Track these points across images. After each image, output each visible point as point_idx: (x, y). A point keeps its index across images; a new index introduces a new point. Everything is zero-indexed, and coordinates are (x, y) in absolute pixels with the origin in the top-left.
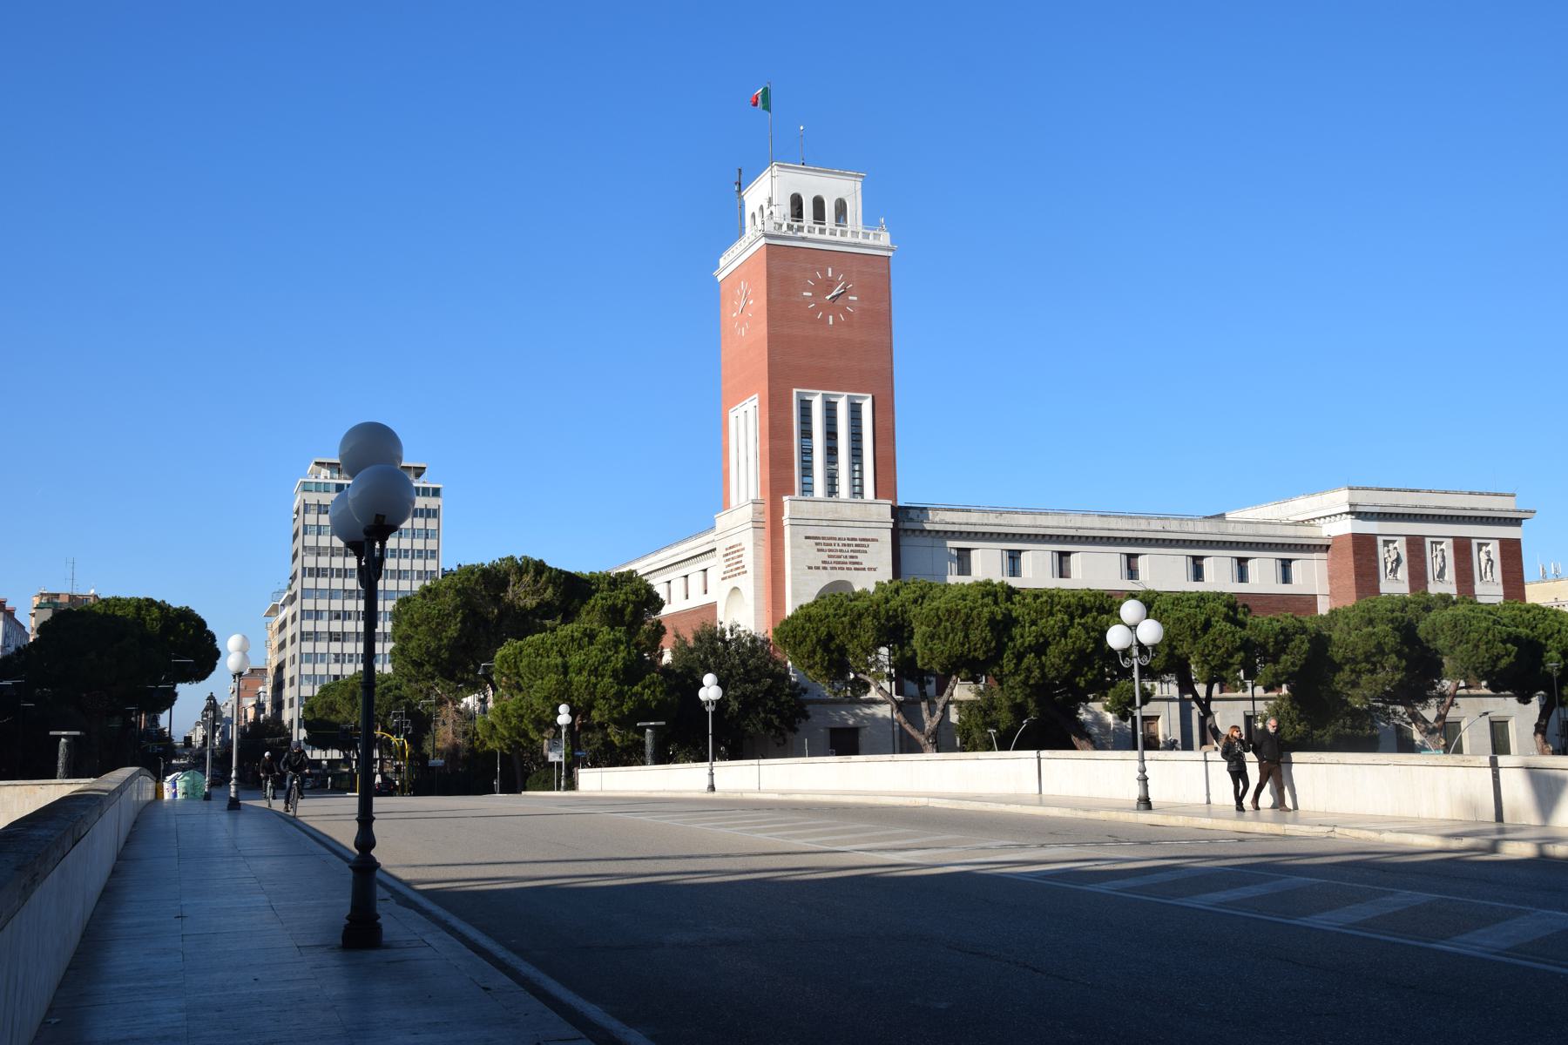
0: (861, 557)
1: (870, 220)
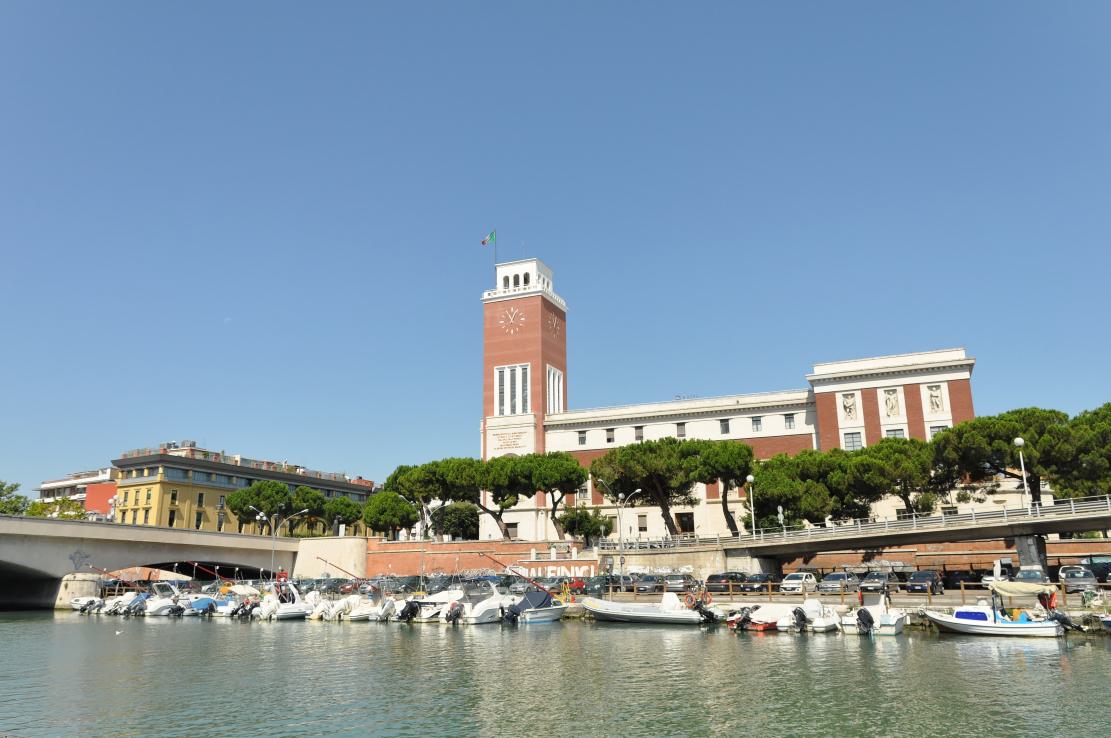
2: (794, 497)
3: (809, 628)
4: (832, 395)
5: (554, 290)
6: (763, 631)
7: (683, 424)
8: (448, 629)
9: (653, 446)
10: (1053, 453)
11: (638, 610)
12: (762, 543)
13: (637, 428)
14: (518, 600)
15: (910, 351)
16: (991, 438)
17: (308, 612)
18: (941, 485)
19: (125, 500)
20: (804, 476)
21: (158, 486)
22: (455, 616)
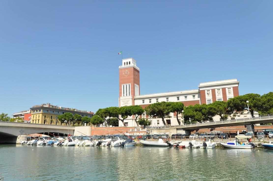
0: (128, 103)
2: (194, 116)
3: (193, 147)
4: (204, 91)
5: (137, 66)
6: (182, 148)
7: (168, 98)
8: (107, 148)
9: (160, 103)
10: (256, 104)
11: (153, 143)
12: (186, 127)
13: (157, 99)
14: (125, 141)
15: (206, 82)
16: (241, 101)
17: (75, 144)
18: (229, 112)
19: (33, 118)
20: (196, 111)
21: (41, 114)
22: (109, 145)
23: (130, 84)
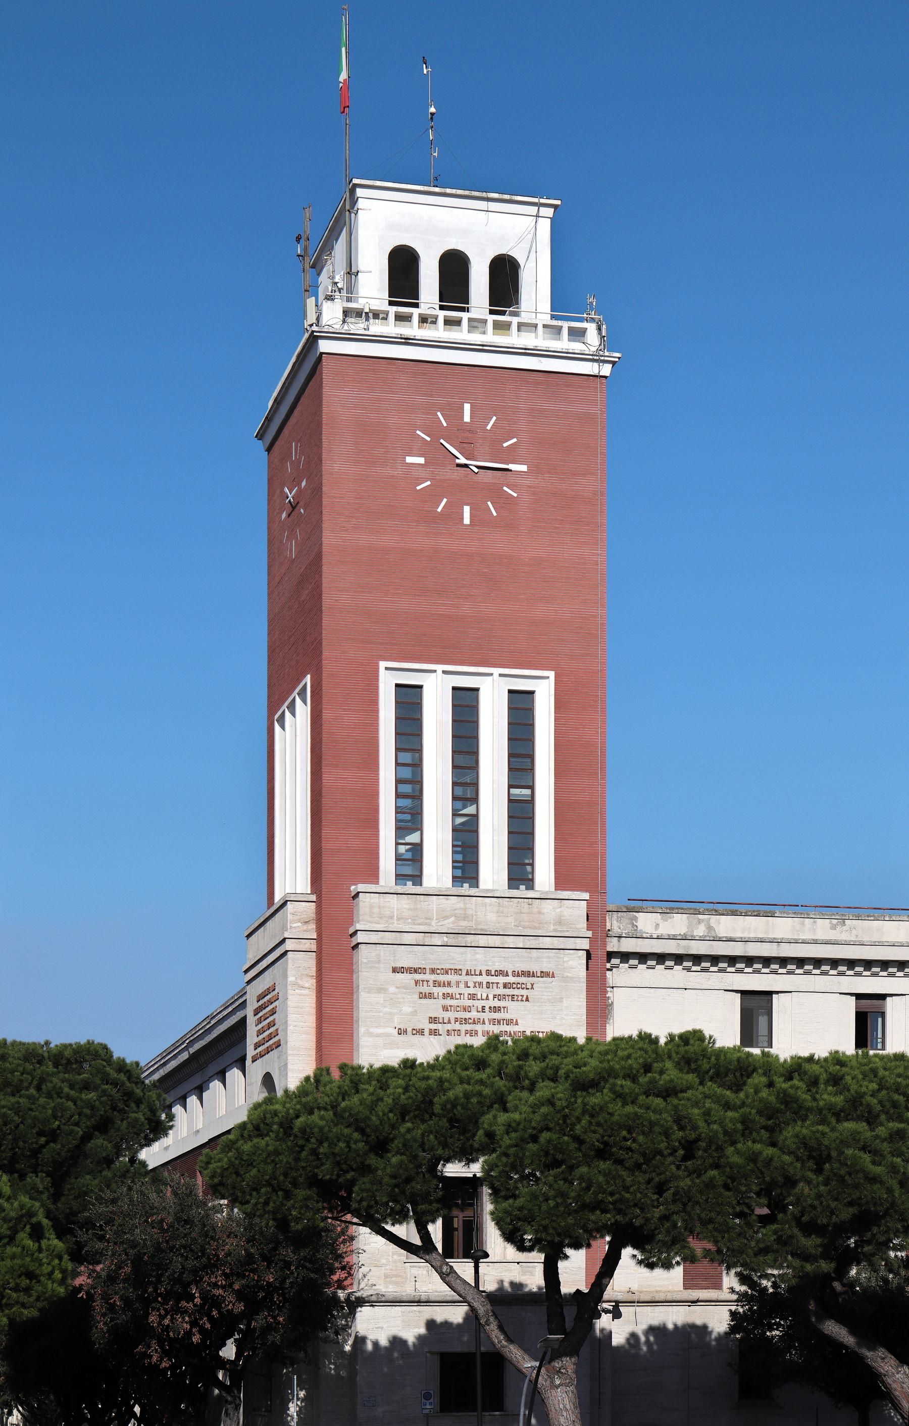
1: (563, 302)
23: (551, 674)
